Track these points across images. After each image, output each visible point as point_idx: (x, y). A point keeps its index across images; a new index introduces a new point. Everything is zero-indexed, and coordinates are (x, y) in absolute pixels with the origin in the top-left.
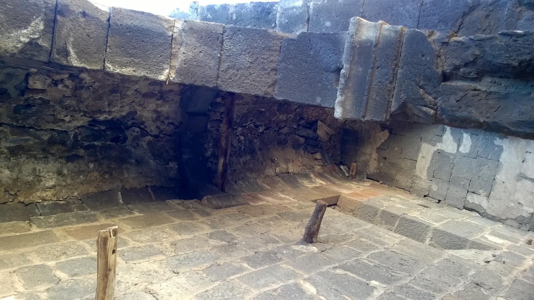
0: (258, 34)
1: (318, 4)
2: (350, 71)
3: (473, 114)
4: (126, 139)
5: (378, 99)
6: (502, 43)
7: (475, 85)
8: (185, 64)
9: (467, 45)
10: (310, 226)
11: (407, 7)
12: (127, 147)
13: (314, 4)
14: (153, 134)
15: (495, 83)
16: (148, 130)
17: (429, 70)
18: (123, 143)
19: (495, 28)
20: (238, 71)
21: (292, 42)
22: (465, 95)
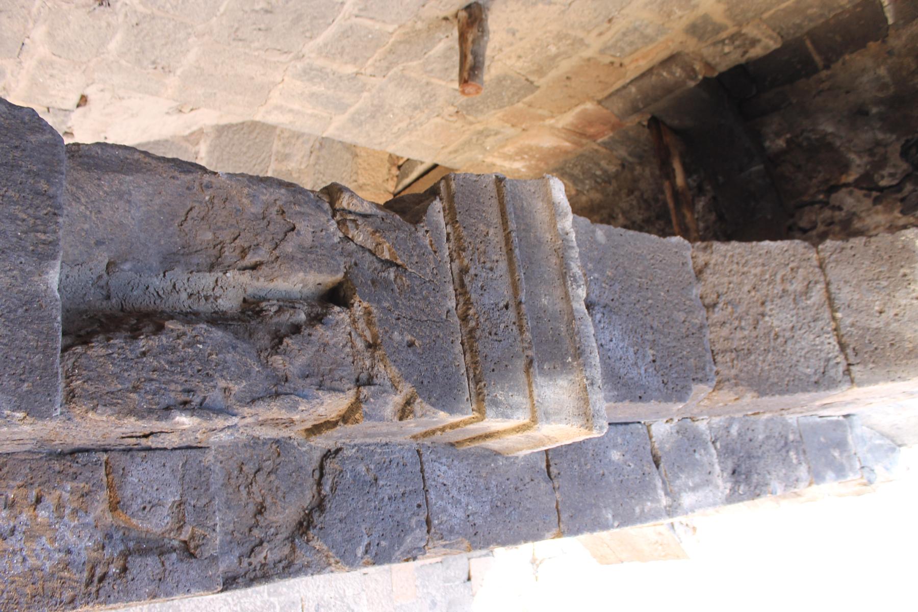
0: (773, 384)
1: (652, 501)
2: (567, 293)
3: (246, 191)
4: (904, 154)
5: (482, 227)
6: (222, 384)
7: (256, 283)
8: (905, 275)
9: (308, 381)
10: (482, 36)
11: (460, 514)
12: (894, 137)
13: (658, 501)
14: (844, 190)
15: (207, 298)
16: (859, 193)
17: (386, 304)
18: (907, 141)
19: (233, 481)
20: (784, 291)
21: (700, 376)
22: (277, 246)
